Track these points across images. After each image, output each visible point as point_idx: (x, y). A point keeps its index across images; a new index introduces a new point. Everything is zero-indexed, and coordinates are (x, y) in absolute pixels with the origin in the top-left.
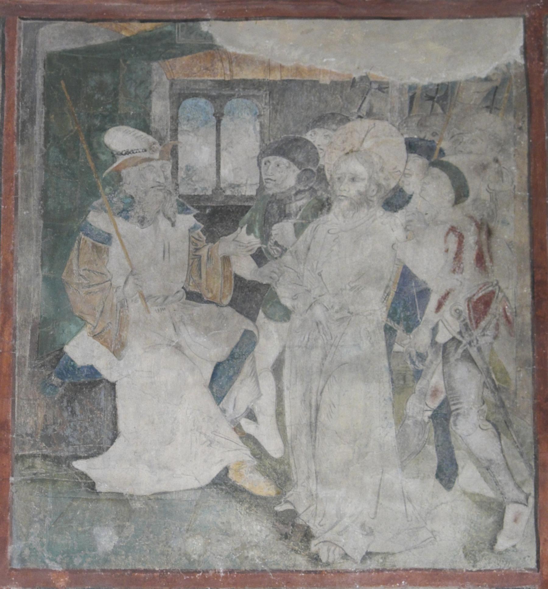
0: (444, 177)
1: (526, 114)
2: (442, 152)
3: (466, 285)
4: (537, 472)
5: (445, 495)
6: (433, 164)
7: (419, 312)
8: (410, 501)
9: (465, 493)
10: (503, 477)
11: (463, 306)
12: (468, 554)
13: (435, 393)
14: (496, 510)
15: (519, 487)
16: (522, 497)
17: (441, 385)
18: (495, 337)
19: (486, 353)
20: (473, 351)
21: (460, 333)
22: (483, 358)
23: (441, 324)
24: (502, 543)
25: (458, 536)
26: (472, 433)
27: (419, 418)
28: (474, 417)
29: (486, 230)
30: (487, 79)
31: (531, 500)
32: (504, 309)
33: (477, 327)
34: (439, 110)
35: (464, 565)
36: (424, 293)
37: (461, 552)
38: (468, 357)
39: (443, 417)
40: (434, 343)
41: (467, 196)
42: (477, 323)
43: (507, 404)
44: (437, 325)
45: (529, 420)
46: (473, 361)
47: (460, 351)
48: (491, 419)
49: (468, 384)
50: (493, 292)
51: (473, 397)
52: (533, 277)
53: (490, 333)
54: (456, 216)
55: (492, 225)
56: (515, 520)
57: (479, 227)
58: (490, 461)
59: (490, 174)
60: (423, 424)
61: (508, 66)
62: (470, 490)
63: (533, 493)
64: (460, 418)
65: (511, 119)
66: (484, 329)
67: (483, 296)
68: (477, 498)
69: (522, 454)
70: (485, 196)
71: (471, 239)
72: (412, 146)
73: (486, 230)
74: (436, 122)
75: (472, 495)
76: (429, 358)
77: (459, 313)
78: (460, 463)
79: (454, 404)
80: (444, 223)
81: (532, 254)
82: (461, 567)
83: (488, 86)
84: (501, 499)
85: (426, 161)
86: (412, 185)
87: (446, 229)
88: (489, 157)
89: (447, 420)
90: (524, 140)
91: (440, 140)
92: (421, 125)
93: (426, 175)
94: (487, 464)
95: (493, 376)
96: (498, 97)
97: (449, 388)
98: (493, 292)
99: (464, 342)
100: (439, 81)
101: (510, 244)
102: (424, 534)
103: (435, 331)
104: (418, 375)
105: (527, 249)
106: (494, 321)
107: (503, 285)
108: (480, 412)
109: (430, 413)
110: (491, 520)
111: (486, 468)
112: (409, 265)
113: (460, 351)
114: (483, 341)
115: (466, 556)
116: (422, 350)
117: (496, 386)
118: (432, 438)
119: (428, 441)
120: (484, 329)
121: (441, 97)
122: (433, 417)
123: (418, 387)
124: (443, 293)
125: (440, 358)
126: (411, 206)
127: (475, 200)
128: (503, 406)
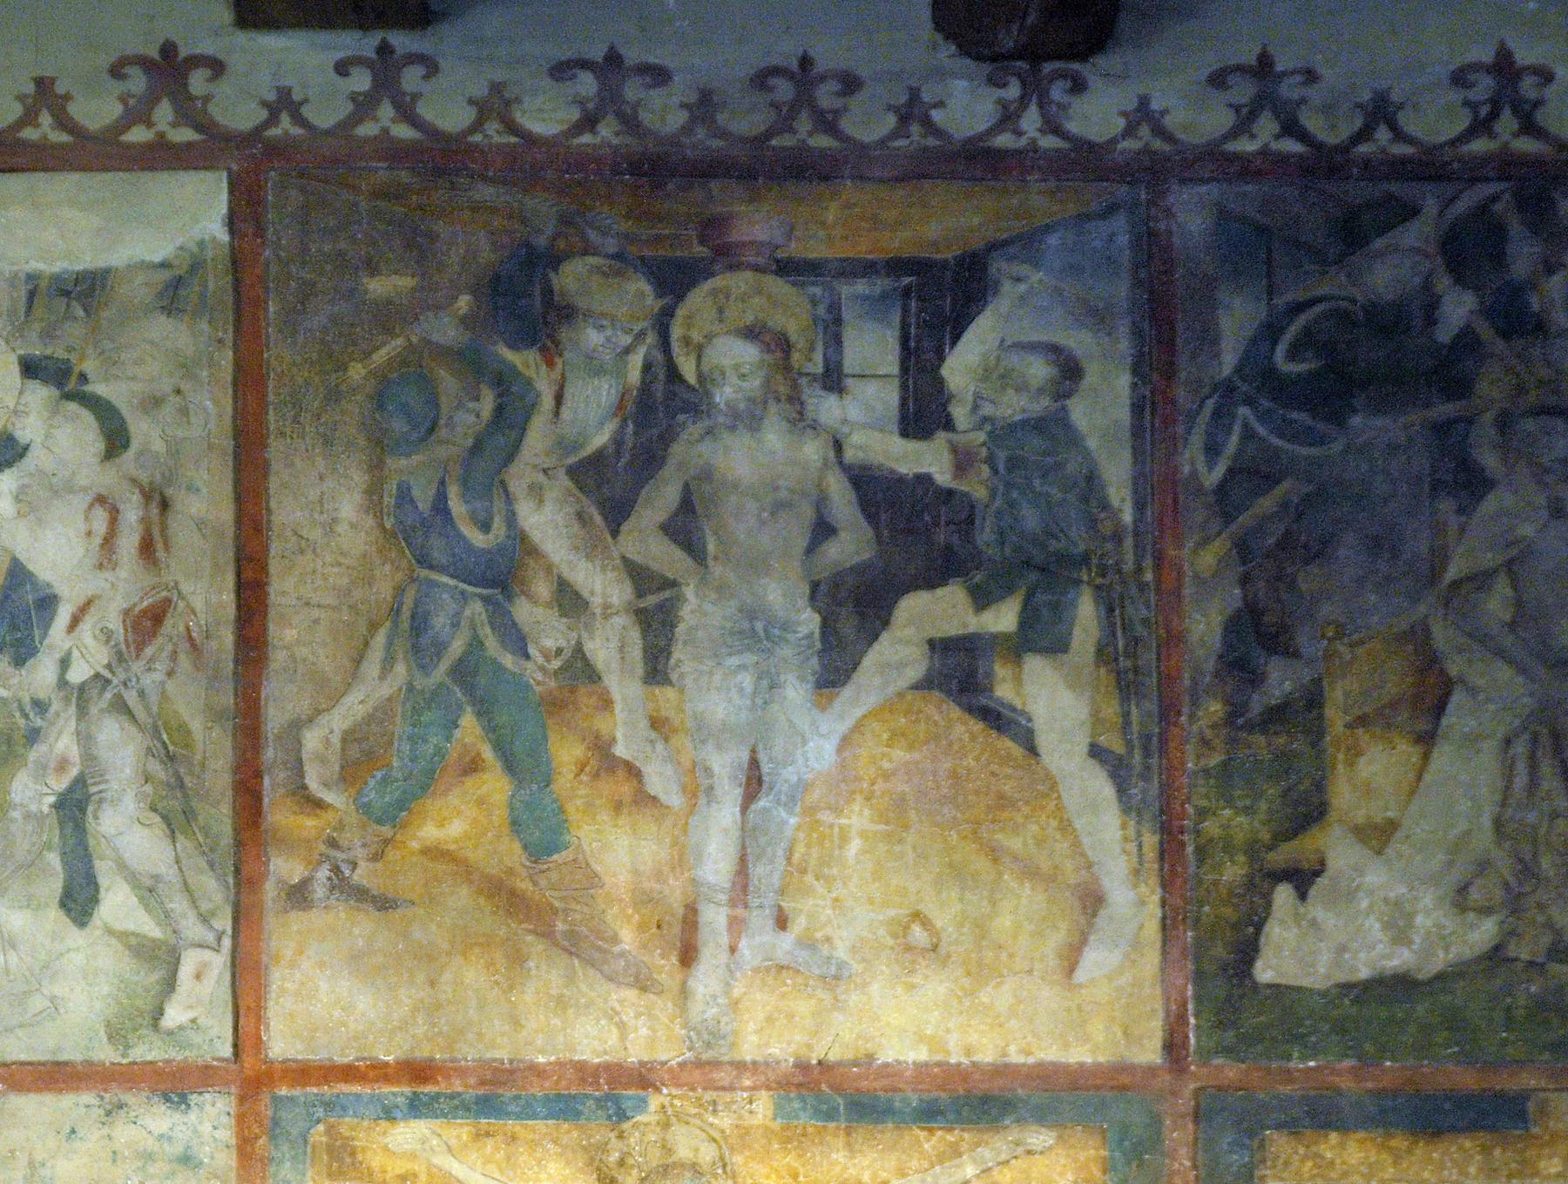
0: (87, 417)
1: (231, 318)
2: (83, 378)
3: (123, 588)
4: (238, 893)
5: (76, 938)
6: (68, 397)
7: (36, 632)
8: (13, 947)
9: (110, 932)
10: (178, 904)
11: (115, 623)
12: (116, 1035)
13: (63, 765)
14: (162, 959)
15: (205, 919)
16: (211, 938)
17: (74, 753)
18: (170, 674)
19: (154, 698)
20: (131, 698)
21: (109, 666)
22: (147, 708)
23: (76, 654)
24: (175, 1015)
25: (98, 1005)
26: (127, 832)
27: (33, 808)
28: (130, 804)
29: (159, 501)
30: (164, 265)
31: (227, 942)
32: (188, 629)
33: (138, 656)
34: (80, 312)
35: (106, 1054)
36: (48, 603)
37: (102, 1033)
38: (120, 707)
39: (74, 807)
40: (62, 683)
41: (126, 445)
42: (140, 648)
43: (188, 780)
44: (69, 653)
45: (226, 809)
46: (132, 717)
47: (108, 695)
48: (159, 806)
49: (121, 750)
50: (168, 601)
51: (128, 771)
52: (238, 574)
53: (161, 666)
54: (107, 478)
55: (169, 492)
56: (198, 977)
57: (147, 496)
58: (157, 878)
59: (168, 411)
60: (40, 818)
61: (201, 244)
62: (118, 926)
63: (229, 932)
64: (104, 806)
65: (205, 326)
66: (152, 660)
67: (152, 606)
68: (133, 941)
69: (211, 865)
70: (158, 446)
71: (132, 514)
72: (30, 369)
73: (159, 501)
74: (74, 331)
75: (123, 936)
76: (53, 709)
77: (108, 635)
78: (103, 881)
79: (95, 784)
80: (84, 489)
81: (237, 537)
82: (102, 1057)
83: (166, 275)
84: (173, 941)
85: (56, 393)
86: (29, 430)
87: (89, 499)
88: (166, 386)
89: (83, 811)
90: (226, 358)
91: (83, 358)
92: (48, 335)
93: (54, 412)
94: (149, 883)
95: (165, 736)
96: (182, 292)
97: (88, 757)
98: (168, 601)
99: (115, 681)
100: (79, 267)
101: (200, 524)
102: (37, 1003)
103: (65, 663)
104: (33, 736)
105: (230, 531)
106: (170, 647)
107: (186, 587)
108: (140, 796)
109: (52, 799)
110: (155, 976)
111: (149, 891)
112: (22, 558)
113: (108, 695)
114: (148, 680)
115: (110, 1038)
116: (42, 695)
117: (169, 750)
118: (56, 840)
119: (48, 846)
120: (152, 660)
121: (85, 290)
122: (59, 806)
123: (33, 755)
124: (81, 601)
125: (73, 709)
126: (29, 462)
127: (140, 453)
128: (182, 785)
